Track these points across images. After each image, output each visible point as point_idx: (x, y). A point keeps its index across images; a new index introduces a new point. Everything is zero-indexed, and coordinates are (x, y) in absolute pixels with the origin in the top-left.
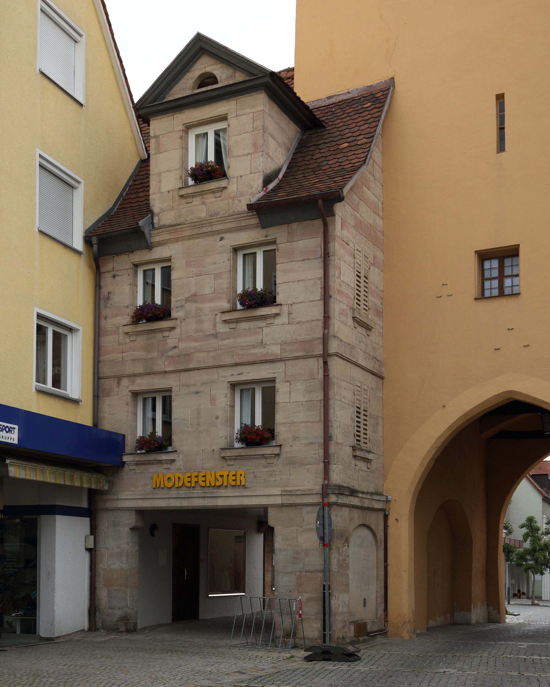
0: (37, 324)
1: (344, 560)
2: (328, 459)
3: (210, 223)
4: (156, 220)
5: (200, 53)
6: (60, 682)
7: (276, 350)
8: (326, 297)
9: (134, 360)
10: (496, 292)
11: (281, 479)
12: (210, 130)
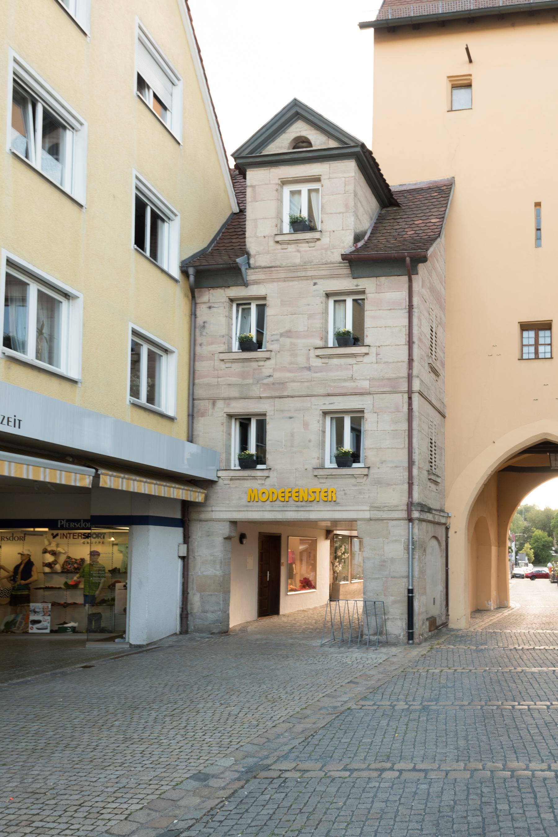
0: (132, 340)
1: (423, 567)
2: (412, 481)
3: (304, 268)
4: (252, 261)
5: (296, 118)
6: (165, 716)
7: (366, 384)
8: (410, 343)
9: (229, 385)
10: (532, 356)
11: (369, 497)
12: (304, 188)
